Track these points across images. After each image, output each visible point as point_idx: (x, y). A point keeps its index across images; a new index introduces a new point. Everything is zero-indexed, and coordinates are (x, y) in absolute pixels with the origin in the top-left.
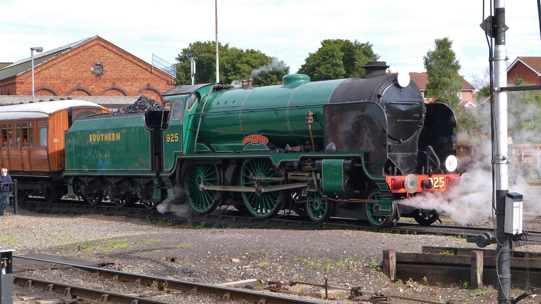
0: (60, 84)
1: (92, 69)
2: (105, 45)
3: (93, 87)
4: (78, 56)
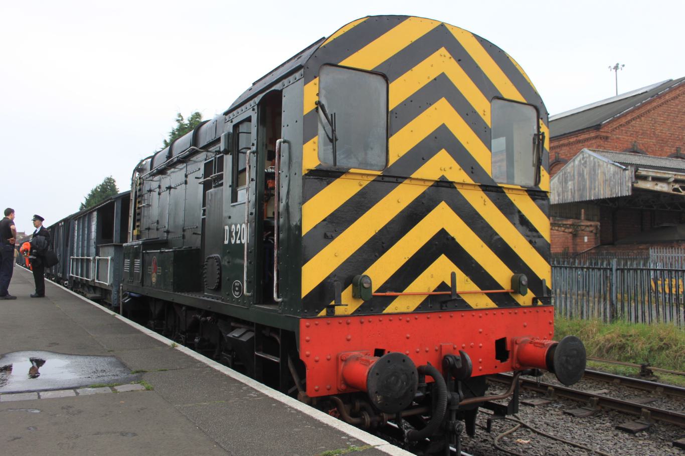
0: (655, 145)
4: (677, 101)
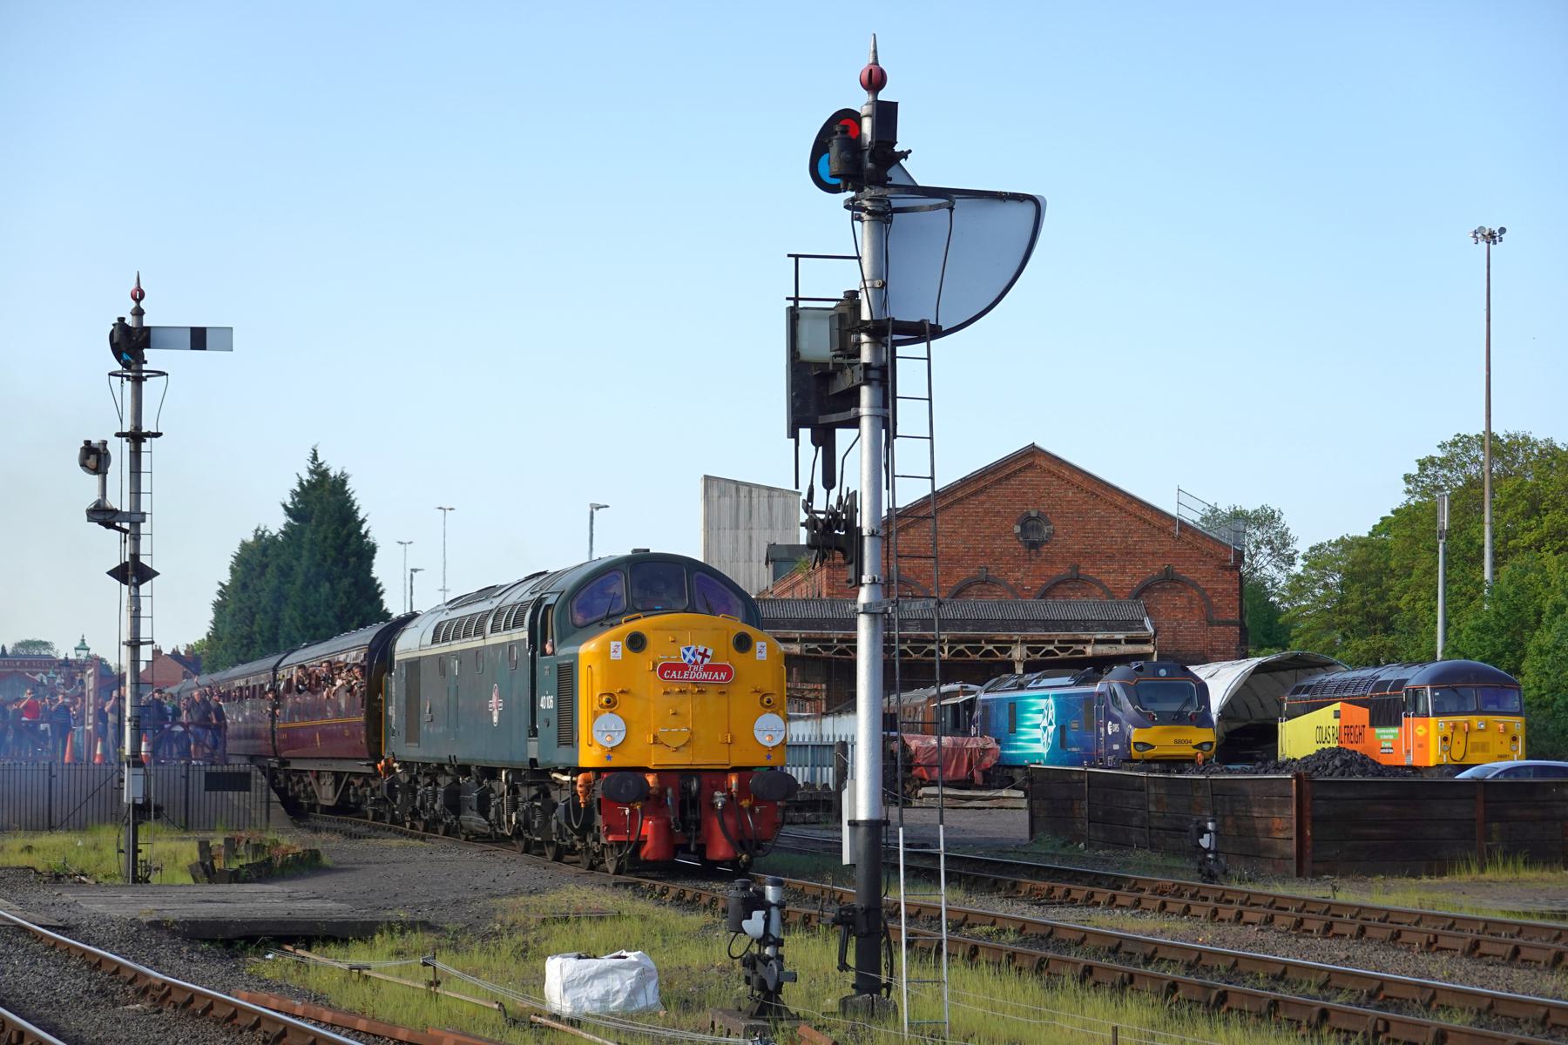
1: (1017, 529)
2: (1053, 468)
3: (1019, 575)
4: (982, 498)
